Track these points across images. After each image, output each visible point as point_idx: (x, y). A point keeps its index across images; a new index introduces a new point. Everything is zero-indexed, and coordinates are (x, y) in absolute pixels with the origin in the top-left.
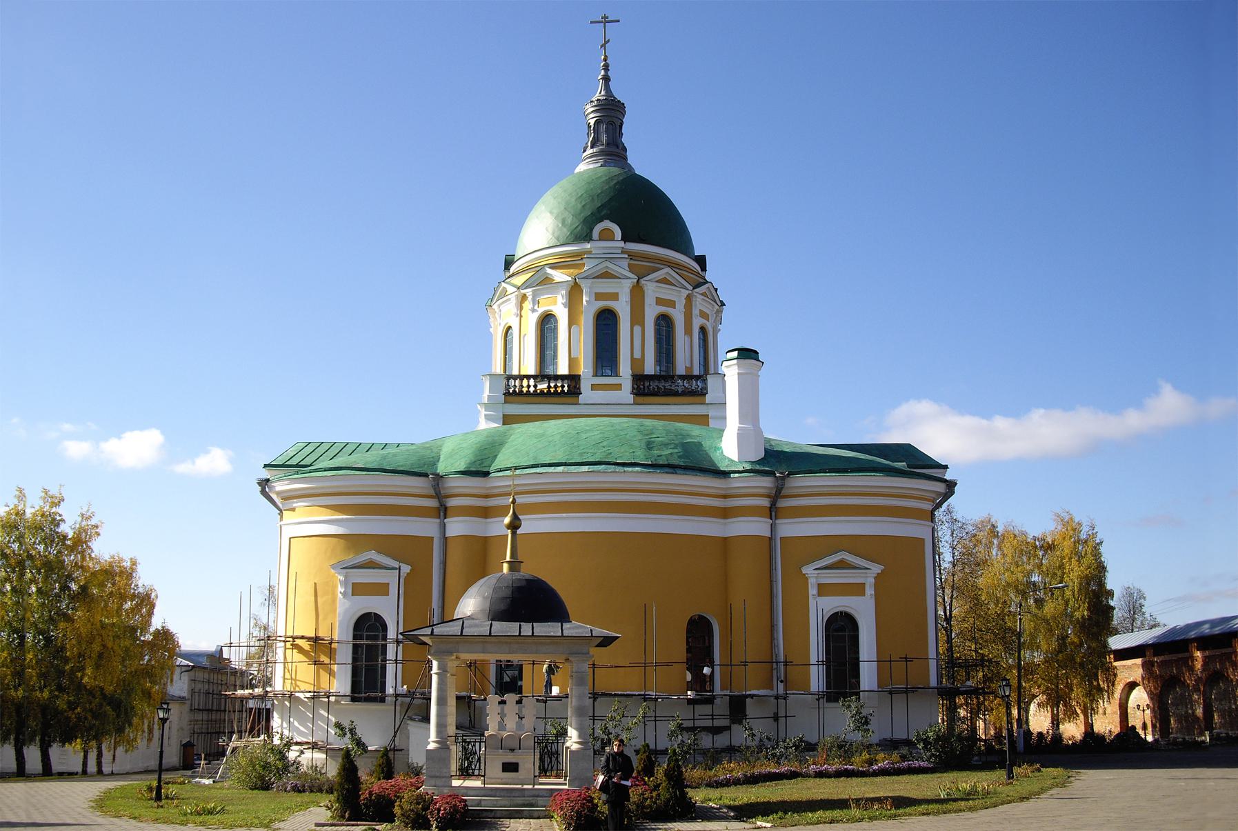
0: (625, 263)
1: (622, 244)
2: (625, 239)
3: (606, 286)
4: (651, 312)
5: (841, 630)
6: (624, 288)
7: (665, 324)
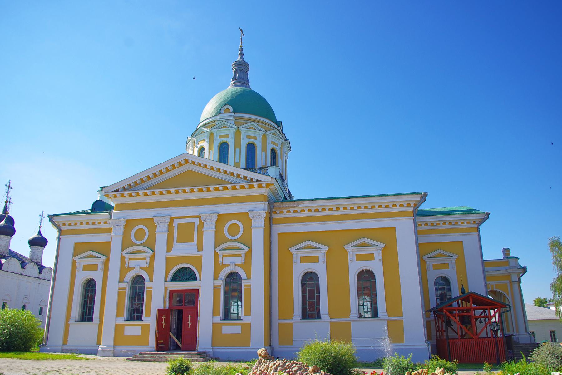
0: (233, 122)
1: (233, 114)
2: (235, 111)
3: (223, 132)
4: (244, 143)
5: (310, 281)
6: (231, 132)
7: (251, 148)
